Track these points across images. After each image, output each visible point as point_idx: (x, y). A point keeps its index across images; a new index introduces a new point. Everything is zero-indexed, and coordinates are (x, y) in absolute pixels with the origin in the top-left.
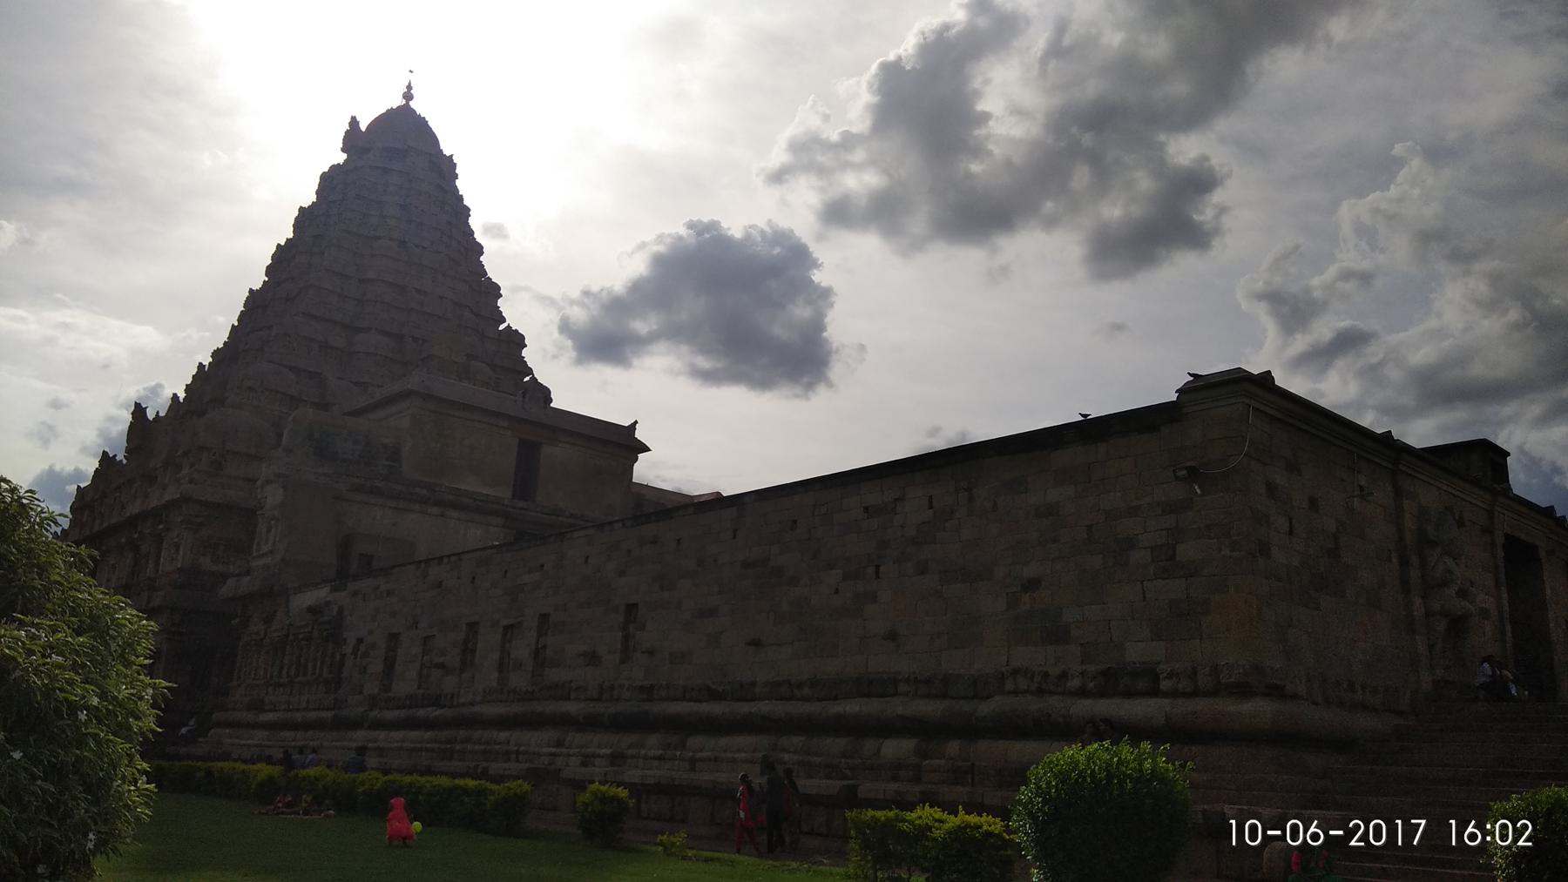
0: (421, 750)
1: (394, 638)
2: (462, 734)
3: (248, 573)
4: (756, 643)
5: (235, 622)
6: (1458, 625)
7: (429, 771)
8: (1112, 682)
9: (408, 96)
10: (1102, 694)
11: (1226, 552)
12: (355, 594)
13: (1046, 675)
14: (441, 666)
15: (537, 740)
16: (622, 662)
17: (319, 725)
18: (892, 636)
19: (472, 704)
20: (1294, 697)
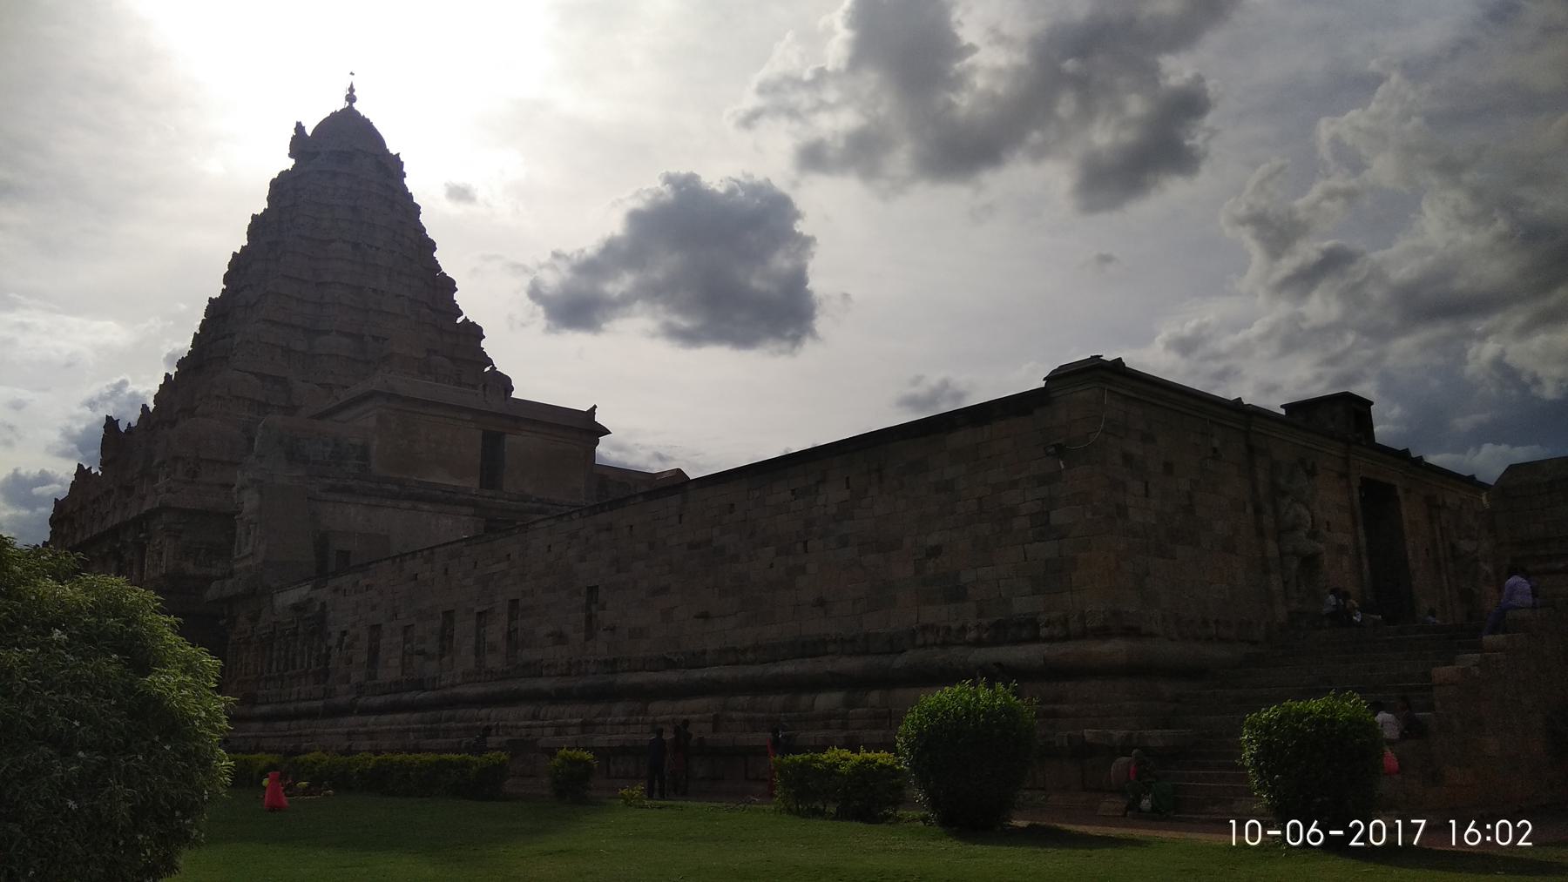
0: (408, 730)
2: (446, 713)
3: (231, 575)
4: (705, 616)
8: (1002, 632)
9: (351, 98)
10: (994, 642)
11: (1089, 516)
12: (336, 590)
13: (949, 628)
14: (422, 653)
15: (512, 715)
16: (587, 639)
17: (311, 715)
18: (821, 603)
19: (453, 686)
20: (1151, 635)
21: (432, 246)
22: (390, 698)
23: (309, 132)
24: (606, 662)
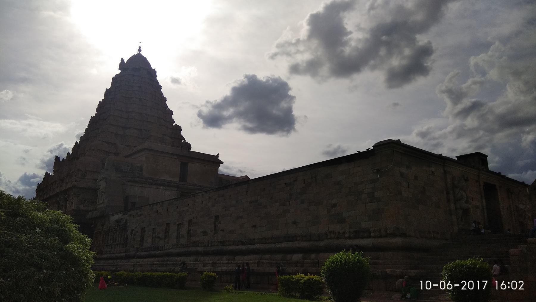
1: (143, 229)
2: (166, 258)
3: (96, 210)
4: (254, 227)
5: (92, 226)
6: (466, 212)
7: (156, 271)
8: (357, 234)
9: (140, 50)
10: (355, 237)
11: (388, 194)
12: (130, 215)
13: (339, 233)
14: (158, 237)
15: (189, 260)
17: (121, 258)
18: (295, 223)
21: (165, 99)
22: (147, 253)
23: (125, 62)
24: (221, 242)
